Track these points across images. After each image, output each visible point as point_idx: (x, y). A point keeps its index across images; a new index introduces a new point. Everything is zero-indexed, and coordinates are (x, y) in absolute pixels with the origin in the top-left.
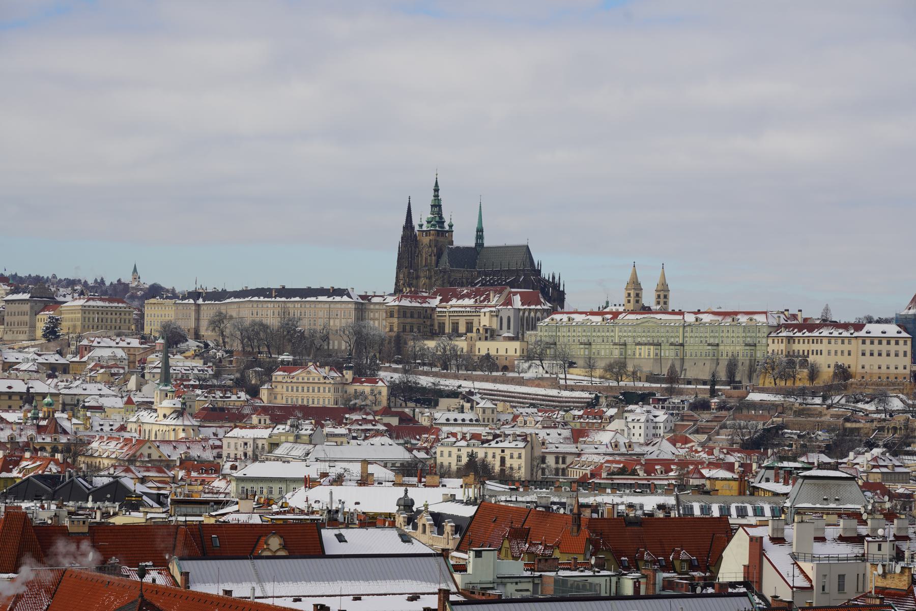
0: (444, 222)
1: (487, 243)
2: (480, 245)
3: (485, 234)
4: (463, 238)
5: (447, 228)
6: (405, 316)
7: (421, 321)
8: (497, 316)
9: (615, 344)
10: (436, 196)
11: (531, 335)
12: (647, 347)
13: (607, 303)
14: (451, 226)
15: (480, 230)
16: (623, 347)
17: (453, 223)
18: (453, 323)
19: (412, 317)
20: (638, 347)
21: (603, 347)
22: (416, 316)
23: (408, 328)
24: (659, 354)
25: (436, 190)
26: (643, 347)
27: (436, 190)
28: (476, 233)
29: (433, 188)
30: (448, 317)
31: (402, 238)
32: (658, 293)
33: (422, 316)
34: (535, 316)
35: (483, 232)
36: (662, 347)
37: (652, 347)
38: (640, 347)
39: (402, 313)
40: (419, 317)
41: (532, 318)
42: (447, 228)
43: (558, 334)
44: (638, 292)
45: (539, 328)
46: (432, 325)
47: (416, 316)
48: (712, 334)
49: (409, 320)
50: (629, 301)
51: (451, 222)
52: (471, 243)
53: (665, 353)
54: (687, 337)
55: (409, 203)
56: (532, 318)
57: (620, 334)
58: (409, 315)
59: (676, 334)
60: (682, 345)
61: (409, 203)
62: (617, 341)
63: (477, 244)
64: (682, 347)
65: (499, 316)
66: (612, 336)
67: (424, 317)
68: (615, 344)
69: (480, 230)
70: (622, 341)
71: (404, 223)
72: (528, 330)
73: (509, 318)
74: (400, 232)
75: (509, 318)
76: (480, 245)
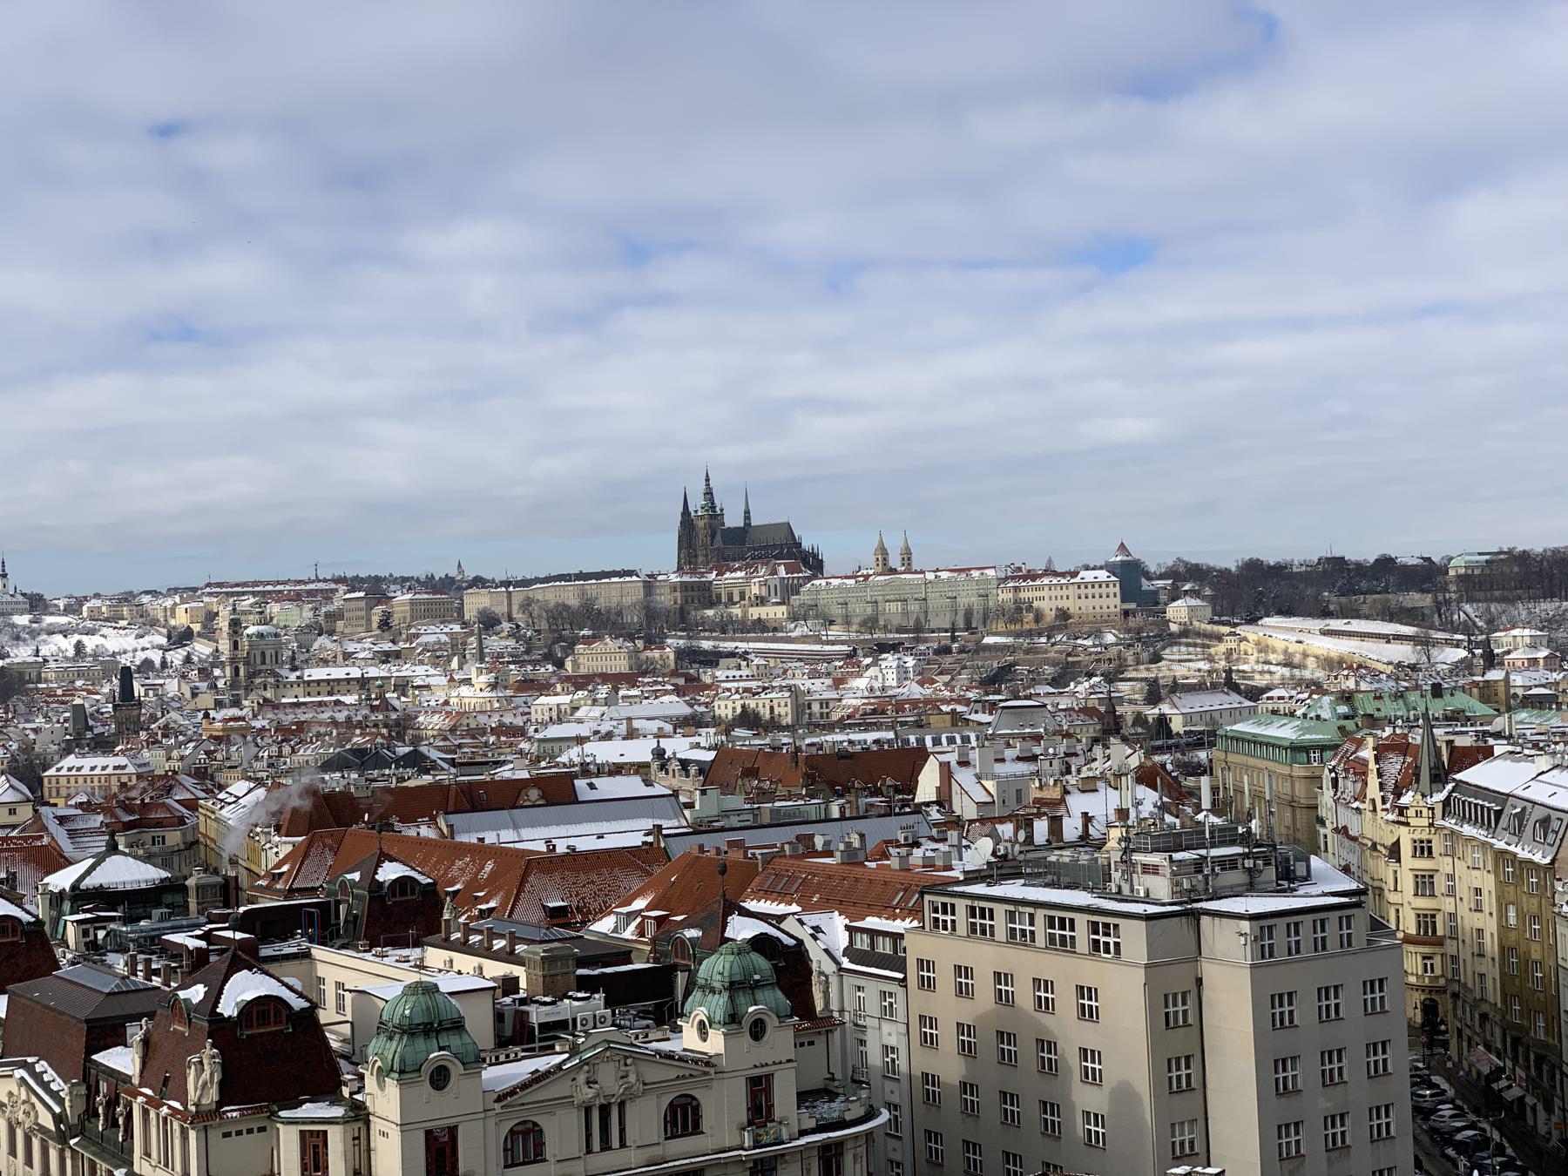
4: (733, 520)
5: (719, 512)
6: (686, 590)
9: (868, 603)
14: (722, 510)
15: (747, 512)
19: (692, 590)
23: (690, 600)
25: (707, 480)
27: (707, 480)
42: (719, 512)
46: (710, 596)
49: (690, 593)
50: (878, 565)
52: (741, 524)
60: (925, 599)
68: (868, 603)
69: (747, 512)
71: (681, 509)
74: (679, 518)
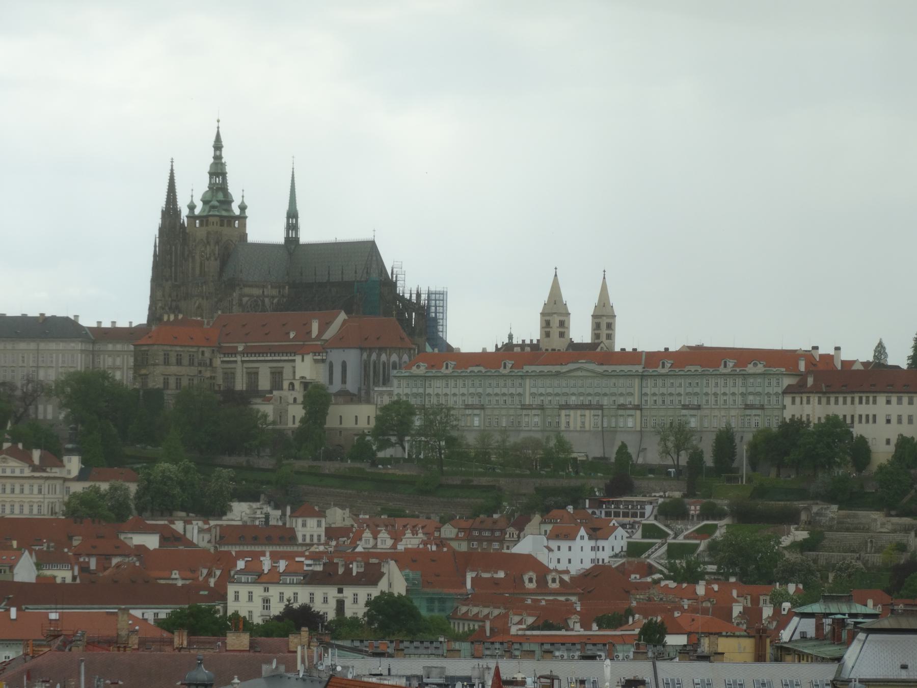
0: (232, 201)
1: (307, 236)
2: (292, 241)
3: (302, 222)
5: (237, 211)
7: (193, 370)
8: (323, 361)
10: (218, 158)
11: (381, 394)
12: (579, 412)
13: (511, 337)
14: (243, 208)
15: (292, 214)
16: (539, 412)
17: (247, 203)
18: (248, 373)
19: (179, 363)
20: (563, 413)
21: (504, 412)
22: (185, 361)
24: (600, 424)
25: (218, 146)
26: (572, 412)
27: (218, 146)
28: (285, 220)
29: (213, 143)
30: (239, 363)
31: (161, 230)
32: (598, 320)
33: (196, 363)
36: (606, 412)
37: (587, 412)
38: (567, 412)
39: (162, 358)
40: (191, 364)
41: (384, 364)
43: (428, 391)
44: (562, 318)
45: (395, 382)
47: (185, 361)
48: (689, 390)
49: (174, 369)
50: (548, 335)
51: (243, 202)
52: (277, 236)
54: (646, 394)
55: (172, 170)
56: (384, 364)
57: (534, 390)
58: (173, 360)
59: (629, 390)
60: (638, 407)
61: (172, 170)
63: (287, 239)
64: (638, 412)
65: (328, 361)
66: (519, 394)
67: (200, 364)
69: (292, 214)
70: (537, 401)
71: (161, 202)
72: (379, 386)
73: (344, 365)
75: (344, 365)
76: (292, 241)
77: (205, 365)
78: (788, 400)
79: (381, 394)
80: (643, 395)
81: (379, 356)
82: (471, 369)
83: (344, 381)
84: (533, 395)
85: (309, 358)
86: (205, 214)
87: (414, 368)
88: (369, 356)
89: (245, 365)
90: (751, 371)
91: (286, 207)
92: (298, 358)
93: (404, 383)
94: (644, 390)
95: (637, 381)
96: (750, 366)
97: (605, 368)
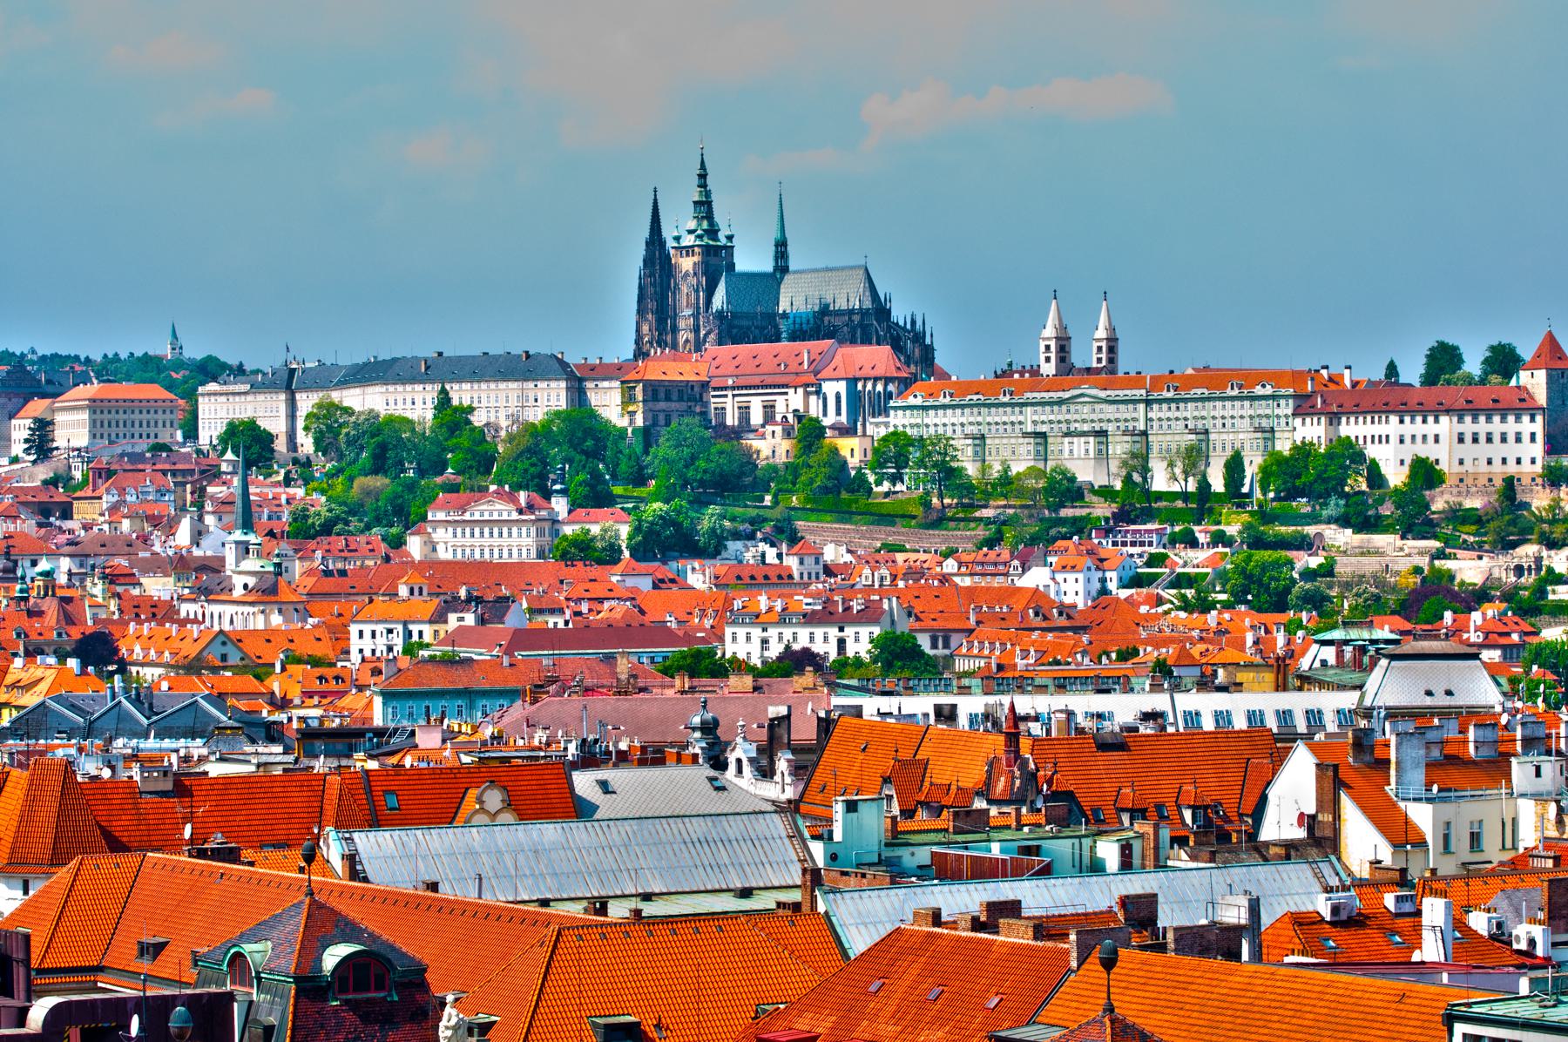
3: (791, 249)
5: (723, 241)
8: (818, 393)
9: (1026, 435)
11: (877, 425)
12: (1083, 439)
13: (1010, 365)
14: (730, 238)
18: (740, 408)
19: (668, 399)
20: (1067, 440)
22: (675, 396)
24: (1104, 452)
25: (703, 176)
26: (1075, 439)
27: (703, 176)
30: (730, 396)
33: (685, 398)
34: (885, 389)
35: (786, 246)
36: (1110, 439)
37: (1091, 439)
38: (1070, 439)
39: (650, 393)
40: (681, 399)
45: (892, 413)
47: (675, 396)
48: (1196, 414)
49: (662, 405)
50: (1048, 360)
53: (1114, 449)
54: (1151, 420)
57: (1036, 418)
58: (662, 395)
60: (1144, 433)
62: (1029, 430)
63: (776, 268)
66: (1020, 423)
68: (1026, 435)
71: (646, 233)
74: (640, 251)
77: (695, 400)
78: (1298, 421)
79: (877, 425)
80: (1148, 420)
81: (874, 386)
82: (969, 397)
83: (838, 413)
84: (1035, 423)
85: (800, 391)
86: (691, 243)
87: (911, 398)
88: (864, 386)
89: (737, 399)
90: (1260, 393)
91: (775, 234)
92: (791, 391)
93: (900, 413)
94: (1150, 415)
95: (1142, 407)
96: (1259, 387)
97: (1108, 392)
